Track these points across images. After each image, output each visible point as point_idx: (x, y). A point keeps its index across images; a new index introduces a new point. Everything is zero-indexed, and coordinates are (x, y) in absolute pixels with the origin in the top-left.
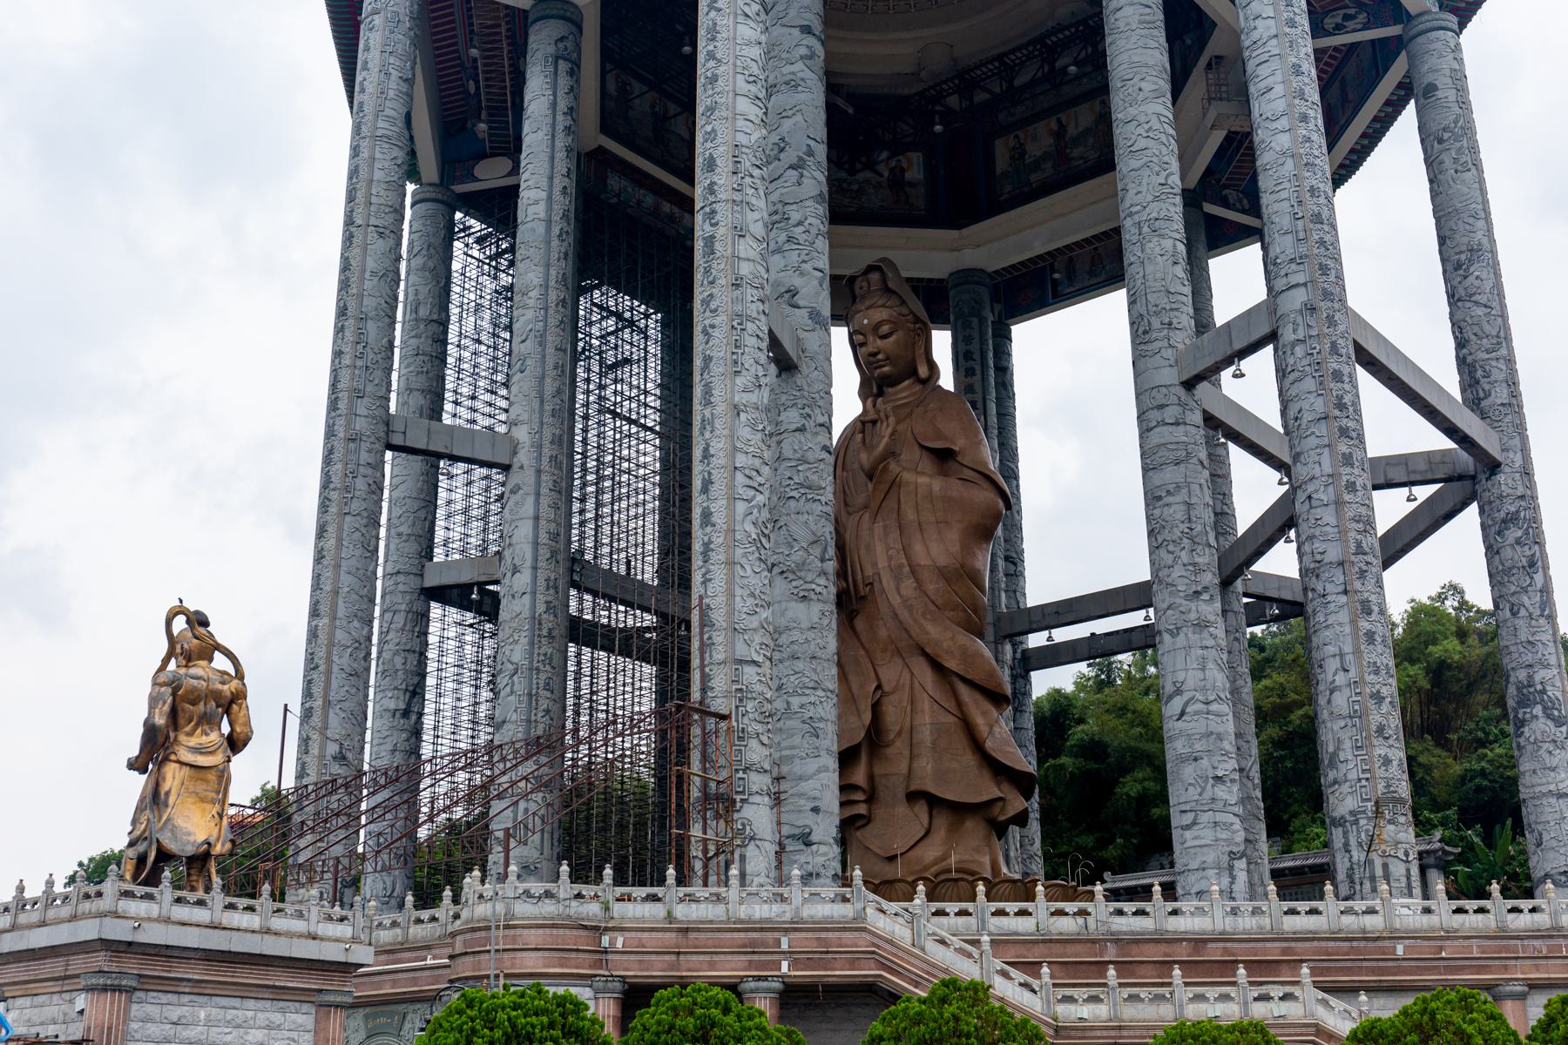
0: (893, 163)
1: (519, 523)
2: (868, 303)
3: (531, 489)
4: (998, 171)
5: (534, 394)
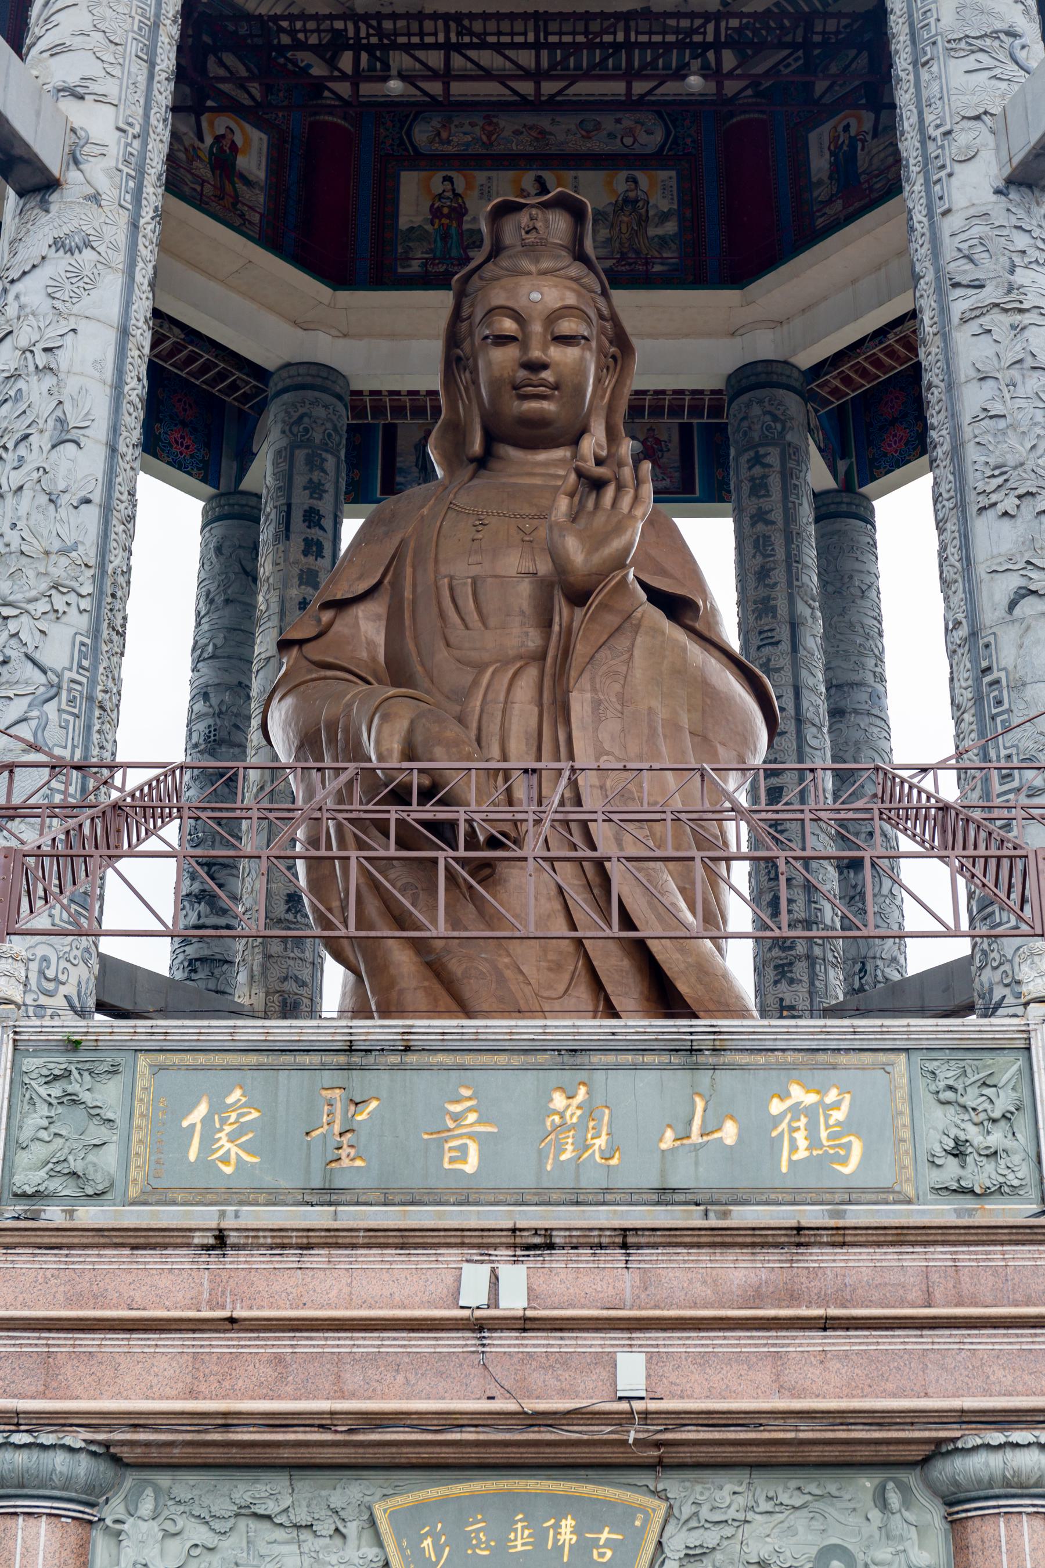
0: (223, 123)
1: (82, 326)
2: (546, 264)
3: (119, 259)
4: (403, 223)
5: (133, 48)
